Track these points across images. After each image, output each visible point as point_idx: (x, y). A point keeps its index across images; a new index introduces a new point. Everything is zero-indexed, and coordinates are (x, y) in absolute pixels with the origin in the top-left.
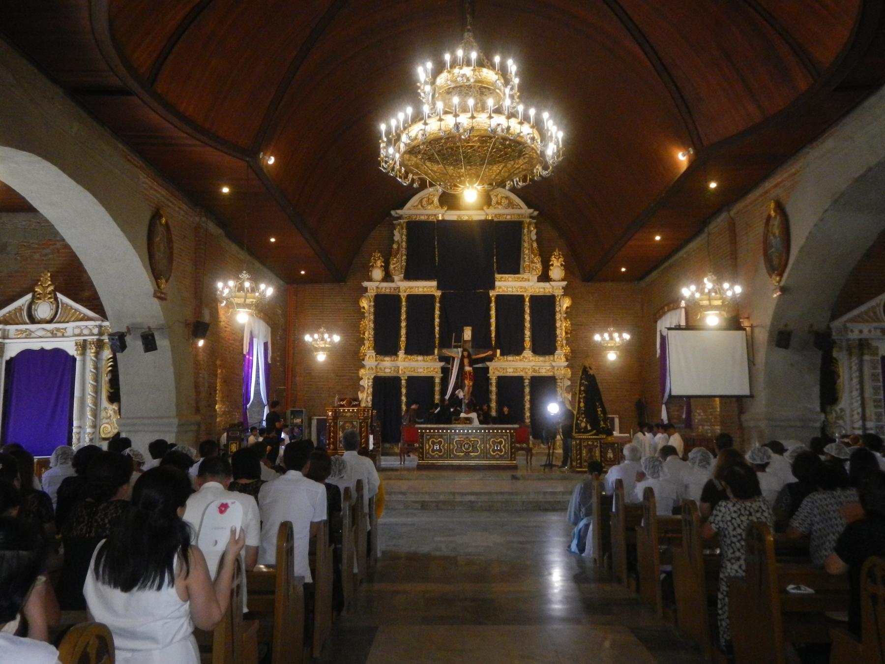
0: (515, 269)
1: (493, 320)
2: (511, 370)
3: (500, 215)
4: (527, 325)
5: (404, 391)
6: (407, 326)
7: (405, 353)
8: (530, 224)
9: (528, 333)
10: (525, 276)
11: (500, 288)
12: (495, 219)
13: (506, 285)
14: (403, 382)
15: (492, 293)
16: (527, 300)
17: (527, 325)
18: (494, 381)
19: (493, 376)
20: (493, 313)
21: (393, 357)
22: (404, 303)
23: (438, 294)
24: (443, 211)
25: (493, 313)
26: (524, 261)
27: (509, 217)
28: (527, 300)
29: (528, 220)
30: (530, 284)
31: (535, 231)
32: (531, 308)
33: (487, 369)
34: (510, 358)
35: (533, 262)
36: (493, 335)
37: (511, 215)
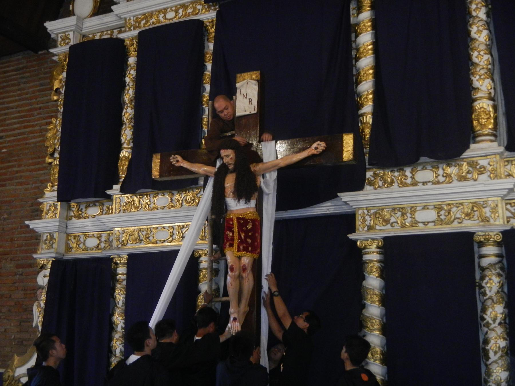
1: (366, 63)
2: (431, 215)
4: (481, 57)
5: (120, 297)
6: (137, 118)
7: (123, 190)
9: (483, 85)
14: (122, 270)
17: (481, 57)
18: (373, 256)
19: (369, 238)
20: (366, 39)
21: (107, 204)
22: (132, 60)
23: (208, 15)
25: (366, 39)
33: (348, 221)
34: (424, 175)
36: (368, 108)
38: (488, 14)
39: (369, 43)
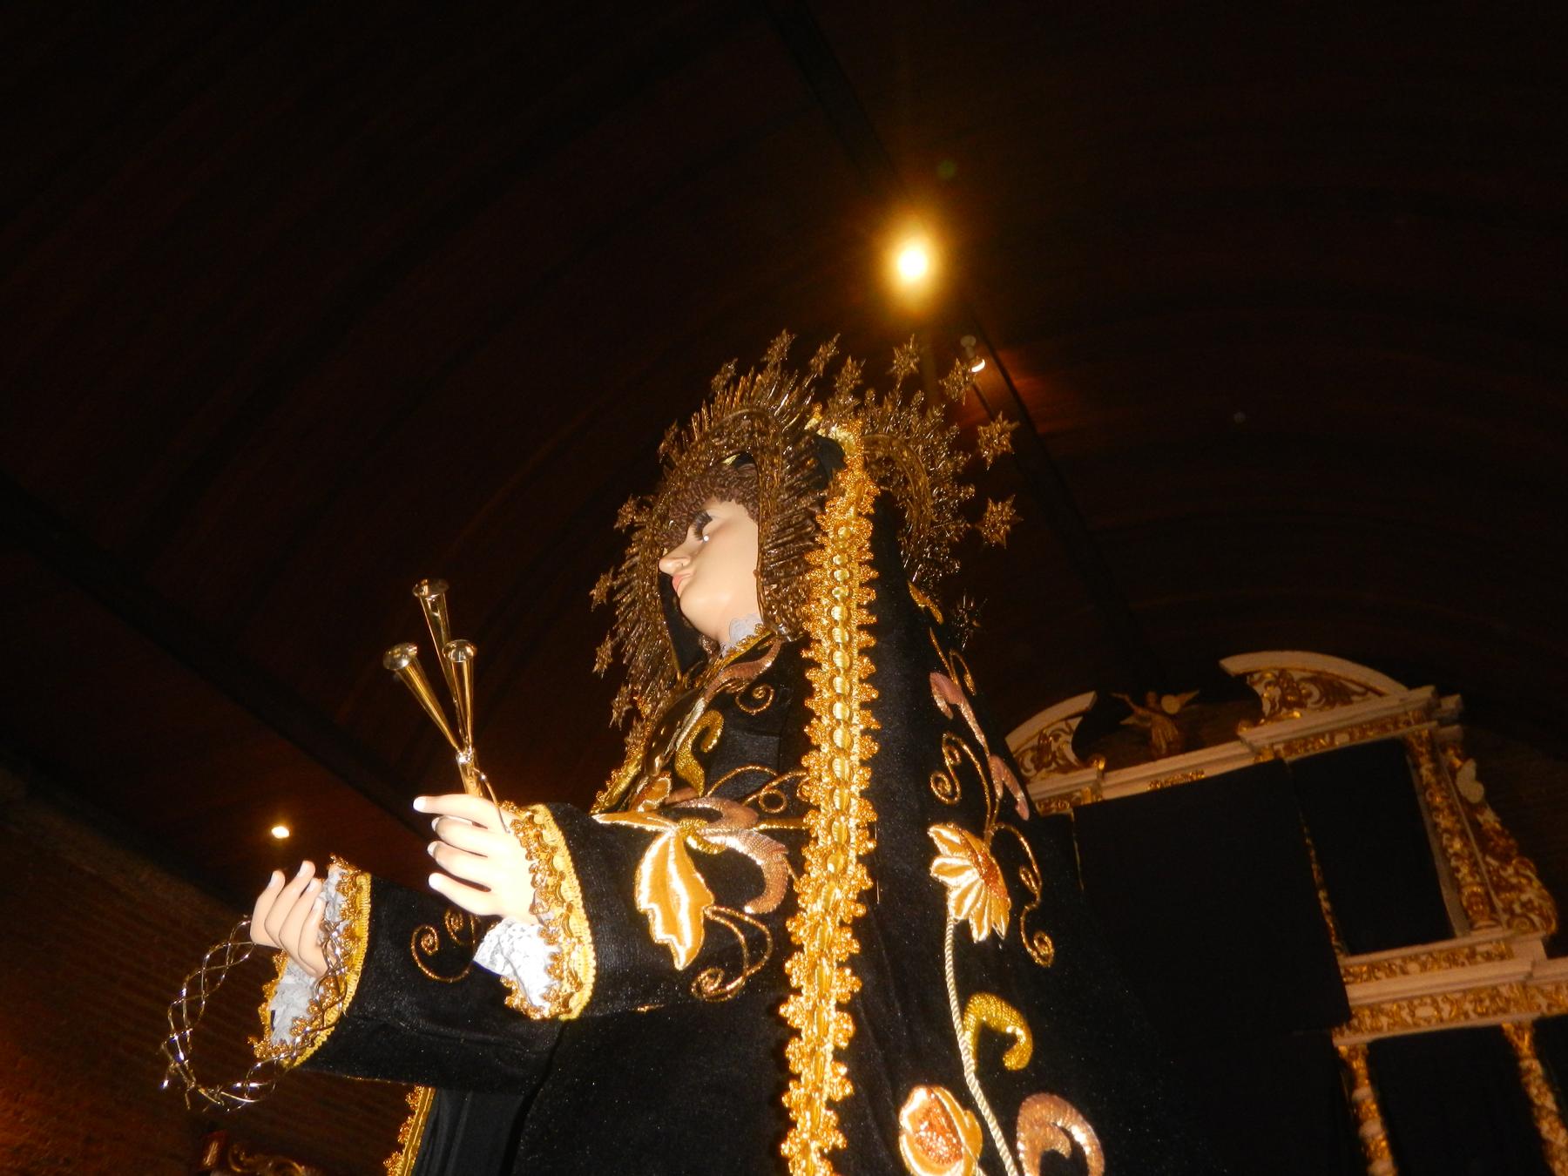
0: (1419, 919)
3: (1305, 741)
8: (1436, 748)
10: (1485, 937)
11: (1375, 1010)
12: (1290, 758)
13: (1398, 993)
15: (1343, 1043)
16: (1525, 1044)
20: (1374, 1130)
24: (1088, 776)
25: (1374, 1130)
26: (1458, 887)
27: (1342, 740)
28: (1525, 1044)
29: (1425, 729)
30: (1514, 969)
31: (1469, 769)
32: (1559, 1081)
35: (1501, 886)
37: (1348, 730)
38: (1557, 1102)
39: (1381, 1137)
